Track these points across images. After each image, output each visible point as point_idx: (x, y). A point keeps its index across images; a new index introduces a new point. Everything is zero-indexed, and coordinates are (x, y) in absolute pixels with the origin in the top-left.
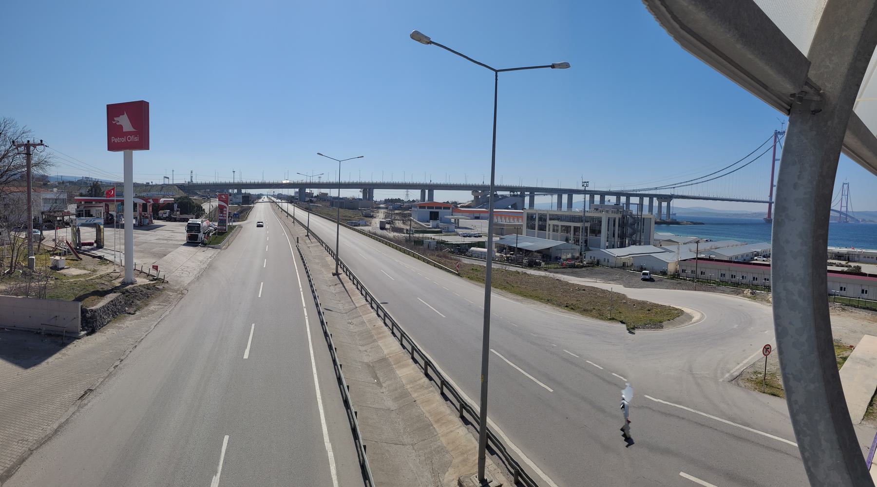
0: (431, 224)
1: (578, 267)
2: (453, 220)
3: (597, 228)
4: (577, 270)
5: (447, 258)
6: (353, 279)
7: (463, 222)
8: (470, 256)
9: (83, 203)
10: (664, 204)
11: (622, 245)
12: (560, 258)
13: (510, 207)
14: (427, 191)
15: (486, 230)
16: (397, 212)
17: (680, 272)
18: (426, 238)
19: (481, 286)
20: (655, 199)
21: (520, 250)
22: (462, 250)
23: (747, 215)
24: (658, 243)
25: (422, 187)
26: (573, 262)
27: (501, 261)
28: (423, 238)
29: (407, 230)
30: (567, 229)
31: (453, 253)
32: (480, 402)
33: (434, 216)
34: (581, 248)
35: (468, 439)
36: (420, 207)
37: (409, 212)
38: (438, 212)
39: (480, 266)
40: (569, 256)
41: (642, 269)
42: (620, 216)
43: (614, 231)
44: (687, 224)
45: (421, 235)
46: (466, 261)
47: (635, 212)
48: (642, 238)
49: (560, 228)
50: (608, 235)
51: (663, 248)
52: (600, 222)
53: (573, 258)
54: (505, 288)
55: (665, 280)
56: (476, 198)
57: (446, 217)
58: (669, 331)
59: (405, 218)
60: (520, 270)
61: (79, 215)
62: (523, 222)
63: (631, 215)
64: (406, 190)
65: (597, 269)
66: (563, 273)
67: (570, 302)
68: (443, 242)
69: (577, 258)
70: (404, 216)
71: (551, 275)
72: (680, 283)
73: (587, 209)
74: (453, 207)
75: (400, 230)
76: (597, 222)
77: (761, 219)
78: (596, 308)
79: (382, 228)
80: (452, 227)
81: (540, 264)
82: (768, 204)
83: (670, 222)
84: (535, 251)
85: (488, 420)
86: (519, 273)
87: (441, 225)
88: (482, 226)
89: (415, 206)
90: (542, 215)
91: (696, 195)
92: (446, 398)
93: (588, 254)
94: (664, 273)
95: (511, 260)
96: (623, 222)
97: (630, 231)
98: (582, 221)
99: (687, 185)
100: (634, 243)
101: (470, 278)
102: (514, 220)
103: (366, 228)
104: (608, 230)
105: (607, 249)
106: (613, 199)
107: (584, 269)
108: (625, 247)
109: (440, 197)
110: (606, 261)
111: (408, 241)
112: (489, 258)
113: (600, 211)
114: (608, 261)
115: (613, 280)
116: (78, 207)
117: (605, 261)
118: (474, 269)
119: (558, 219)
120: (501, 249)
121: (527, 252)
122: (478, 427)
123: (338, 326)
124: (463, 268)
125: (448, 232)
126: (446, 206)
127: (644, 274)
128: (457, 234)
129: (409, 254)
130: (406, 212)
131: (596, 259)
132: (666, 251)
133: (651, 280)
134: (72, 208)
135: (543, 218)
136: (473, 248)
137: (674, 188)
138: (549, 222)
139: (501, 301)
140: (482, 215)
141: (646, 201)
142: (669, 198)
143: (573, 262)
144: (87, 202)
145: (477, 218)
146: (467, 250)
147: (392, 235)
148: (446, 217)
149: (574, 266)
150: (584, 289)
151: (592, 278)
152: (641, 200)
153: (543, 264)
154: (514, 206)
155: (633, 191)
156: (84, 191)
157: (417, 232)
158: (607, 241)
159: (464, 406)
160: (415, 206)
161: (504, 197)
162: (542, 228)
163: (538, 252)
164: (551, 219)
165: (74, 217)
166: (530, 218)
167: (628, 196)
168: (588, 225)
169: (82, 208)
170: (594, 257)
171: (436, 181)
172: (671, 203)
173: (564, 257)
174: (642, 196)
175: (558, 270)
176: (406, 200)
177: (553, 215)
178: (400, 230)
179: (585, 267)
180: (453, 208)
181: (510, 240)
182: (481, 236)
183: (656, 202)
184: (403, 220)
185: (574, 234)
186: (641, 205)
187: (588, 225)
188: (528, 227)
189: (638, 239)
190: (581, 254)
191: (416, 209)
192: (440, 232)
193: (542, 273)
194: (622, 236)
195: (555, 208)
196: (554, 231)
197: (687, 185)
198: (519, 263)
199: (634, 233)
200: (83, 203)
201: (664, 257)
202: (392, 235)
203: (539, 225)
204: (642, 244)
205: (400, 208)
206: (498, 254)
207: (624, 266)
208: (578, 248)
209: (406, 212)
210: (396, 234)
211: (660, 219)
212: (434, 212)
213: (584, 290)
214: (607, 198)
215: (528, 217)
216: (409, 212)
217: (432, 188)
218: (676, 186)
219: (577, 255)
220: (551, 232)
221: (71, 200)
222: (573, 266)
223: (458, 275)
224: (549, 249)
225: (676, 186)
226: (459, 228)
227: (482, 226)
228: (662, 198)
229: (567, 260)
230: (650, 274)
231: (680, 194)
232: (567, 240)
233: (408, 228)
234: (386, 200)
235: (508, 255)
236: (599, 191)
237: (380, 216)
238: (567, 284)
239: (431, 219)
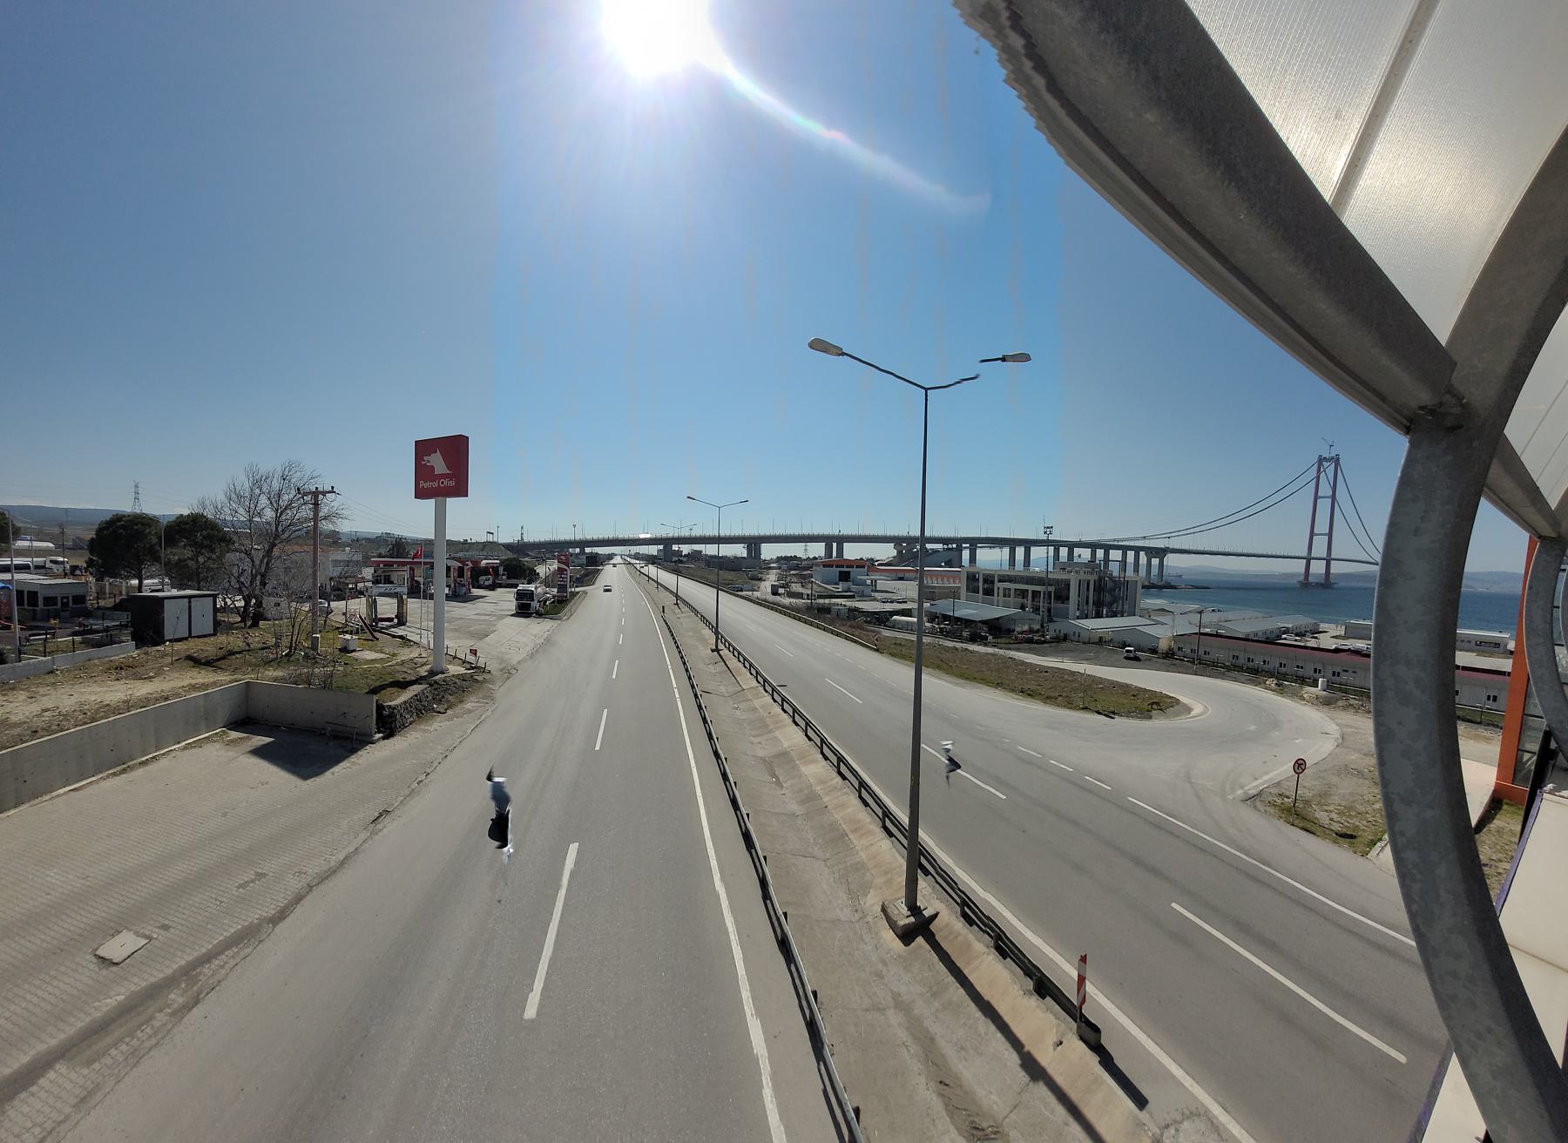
0: (841, 587)
1: (1038, 642)
2: (869, 582)
3: (1064, 593)
4: (1036, 646)
5: (862, 629)
6: (738, 655)
7: (881, 585)
8: (893, 627)
9: (381, 566)
10: (1155, 561)
11: (1099, 615)
12: (1014, 631)
13: (943, 564)
14: (835, 545)
15: (915, 595)
16: (793, 572)
17: (1176, 650)
18: (834, 605)
19: (909, 666)
20: (1142, 554)
21: (958, 619)
22: (882, 619)
24: (1146, 613)
25: (828, 540)
26: (1030, 636)
27: (932, 633)
28: (830, 604)
29: (808, 595)
30: (1023, 593)
31: (870, 622)
32: (908, 811)
33: (844, 577)
34: (1043, 618)
35: (892, 856)
36: (824, 566)
37: (809, 572)
38: (849, 572)
39: (906, 640)
40: (1026, 628)
41: (1124, 645)
42: (1093, 578)
43: (1088, 597)
45: (827, 601)
46: (886, 633)
47: (1116, 574)
48: (1125, 607)
49: (1012, 592)
50: (1079, 601)
51: (1153, 620)
52: (1068, 585)
53: (1031, 631)
54: (939, 667)
55: (1155, 660)
56: (900, 552)
57: (859, 577)
58: (1158, 723)
59: (804, 580)
60: (959, 645)
61: (376, 582)
62: (962, 584)
63: (1111, 577)
64: (804, 544)
65: (1064, 645)
66: (1018, 650)
67: (1026, 687)
68: (856, 610)
69: (1037, 631)
70: (804, 577)
71: (1002, 652)
72: (1174, 665)
73: (1050, 569)
74: (869, 565)
75: (799, 596)
76: (1063, 586)
78: (1064, 694)
79: (775, 593)
80: (868, 591)
81: (986, 638)
83: (1161, 586)
84: (980, 621)
85: (921, 833)
86: (957, 649)
87: (854, 588)
88: (909, 589)
89: (817, 565)
90: (988, 575)
91: (1200, 548)
92: (866, 804)
93: (1052, 626)
94: (1154, 651)
95: (946, 632)
96: (1100, 585)
97: (1108, 598)
98: (1044, 585)
100: (1114, 615)
101: (893, 655)
102: (948, 580)
103: (756, 594)
104: (1079, 596)
105: (1079, 621)
106: (1084, 554)
107: (1046, 645)
108: (1102, 617)
109: (852, 552)
110: (1077, 634)
111: (809, 609)
112: (921, 633)
113: (1068, 572)
114: (1079, 636)
115: (1087, 660)
116: (375, 571)
117: (1074, 635)
118: (898, 644)
119: (1010, 581)
120: (933, 618)
121: (968, 623)
122: (905, 842)
123: (720, 712)
124: (884, 643)
125: (863, 596)
126: (860, 564)
127: (1127, 651)
128: (875, 599)
129: (811, 624)
130: (805, 573)
131: (1062, 632)
132: (1157, 623)
133: (1137, 659)
134: (368, 572)
135: (989, 580)
136: (895, 617)
138: (997, 585)
139: (937, 686)
140: (907, 575)
142: (1161, 553)
143: (1030, 636)
144: (387, 564)
145: (901, 579)
146: (888, 620)
147: (787, 601)
148: (859, 577)
149: (1032, 641)
150: (1046, 670)
151: (1057, 657)
152: (1125, 555)
153: (990, 638)
154: (949, 564)
156: (383, 551)
157: (820, 597)
158: (1078, 609)
159: (887, 814)
160: (817, 565)
161: (935, 551)
162: (989, 592)
163: (984, 622)
164: (999, 581)
165: (370, 584)
166: (972, 578)
168: (1052, 589)
169: (380, 572)
170: (1060, 631)
171: (846, 532)
173: (1018, 629)
175: (1011, 646)
176: (804, 557)
177: (1003, 576)
178: (799, 596)
179: (1048, 643)
180: (869, 567)
181: (944, 606)
182: (906, 602)
184: (802, 583)
185: (1033, 600)
186: (1124, 562)
187: (1052, 589)
188: (968, 589)
189: (1120, 609)
190: (1042, 626)
191: (818, 569)
192: (853, 597)
193: (990, 650)
194: (1099, 604)
195: (1006, 566)
196: (1005, 596)
198: (961, 639)
199: (1115, 600)
200: (381, 566)
201: (1154, 631)
202: (787, 601)
203: (984, 589)
204: (1125, 614)
205: (797, 567)
206: (928, 625)
207: (1101, 642)
208: (1040, 617)
209: (805, 573)
210: (793, 600)
212: (845, 572)
213: (1046, 672)
215: (968, 577)
216: (809, 572)
217: (842, 540)
219: (1037, 627)
220: (1001, 598)
221: (366, 562)
222: (1030, 641)
223: (877, 650)
224: (998, 619)
226: (877, 591)
227: (909, 589)
229: (1022, 633)
230: (1135, 651)
232: (1023, 607)
233: (809, 592)
234: (778, 557)
235: (942, 626)
237: (772, 578)
238: (1023, 663)
239: (840, 580)
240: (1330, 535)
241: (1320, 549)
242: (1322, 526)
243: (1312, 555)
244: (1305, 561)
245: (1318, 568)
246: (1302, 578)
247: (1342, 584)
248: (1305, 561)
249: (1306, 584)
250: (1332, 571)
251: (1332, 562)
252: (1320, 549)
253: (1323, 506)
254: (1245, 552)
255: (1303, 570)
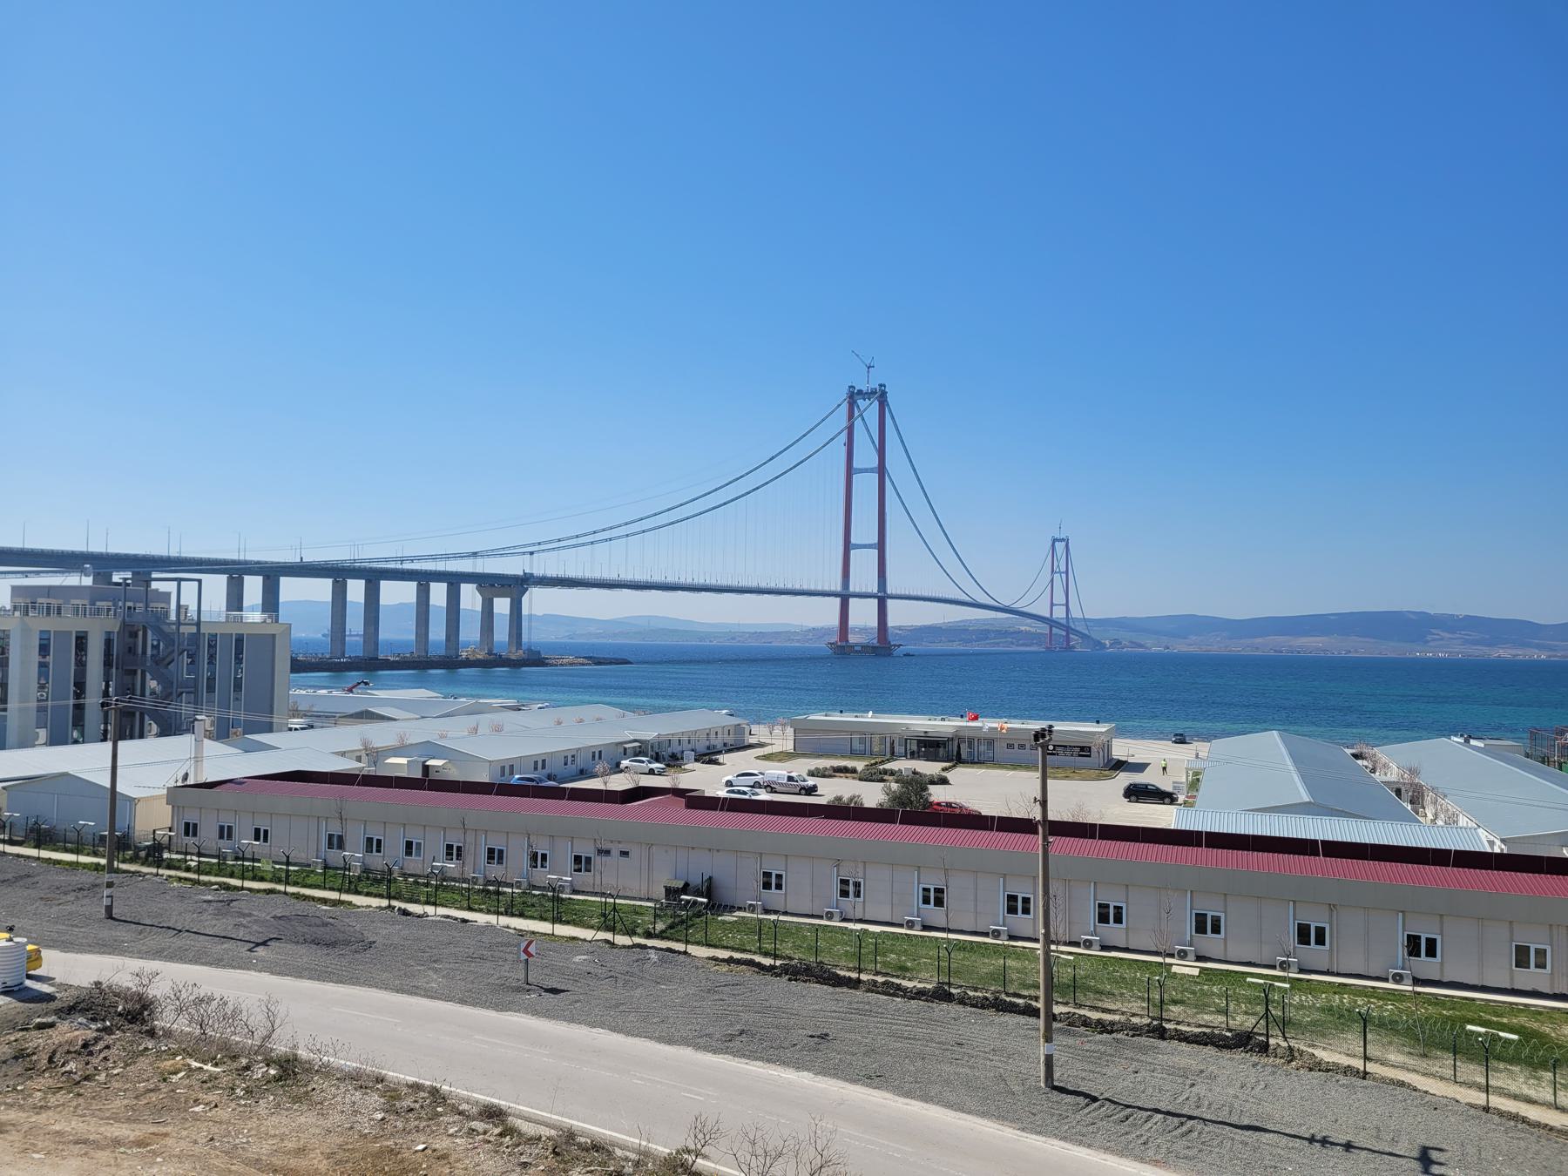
10: (502, 605)
23: (788, 635)
44: (571, 664)
77: (821, 645)
82: (838, 599)
91: (611, 575)
99: (574, 546)
137: (532, 553)
141: (439, 592)
142: (516, 586)
155: (395, 560)
167: (374, 577)
172: (525, 599)
174: (424, 579)
183: (470, 597)
197: (574, 546)
211: (490, 653)
214: (290, 588)
218: (542, 547)
225: (542, 547)
228: (491, 584)
231: (552, 572)
236: (258, 563)
240: (881, 546)
241: (864, 576)
242: (865, 531)
243: (852, 589)
244: (838, 599)
245: (863, 615)
246: (835, 638)
247: (910, 648)
248: (838, 600)
249: (843, 649)
250: (892, 621)
251: (889, 602)
252: (864, 576)
253: (866, 486)
254: (711, 581)
255: (834, 621)
